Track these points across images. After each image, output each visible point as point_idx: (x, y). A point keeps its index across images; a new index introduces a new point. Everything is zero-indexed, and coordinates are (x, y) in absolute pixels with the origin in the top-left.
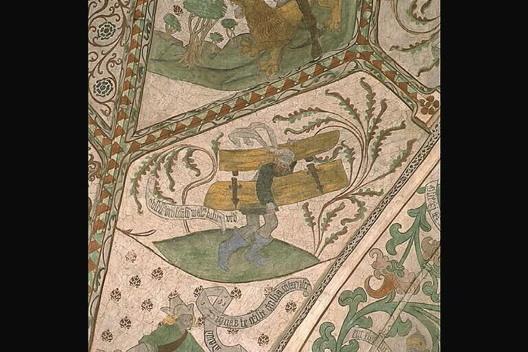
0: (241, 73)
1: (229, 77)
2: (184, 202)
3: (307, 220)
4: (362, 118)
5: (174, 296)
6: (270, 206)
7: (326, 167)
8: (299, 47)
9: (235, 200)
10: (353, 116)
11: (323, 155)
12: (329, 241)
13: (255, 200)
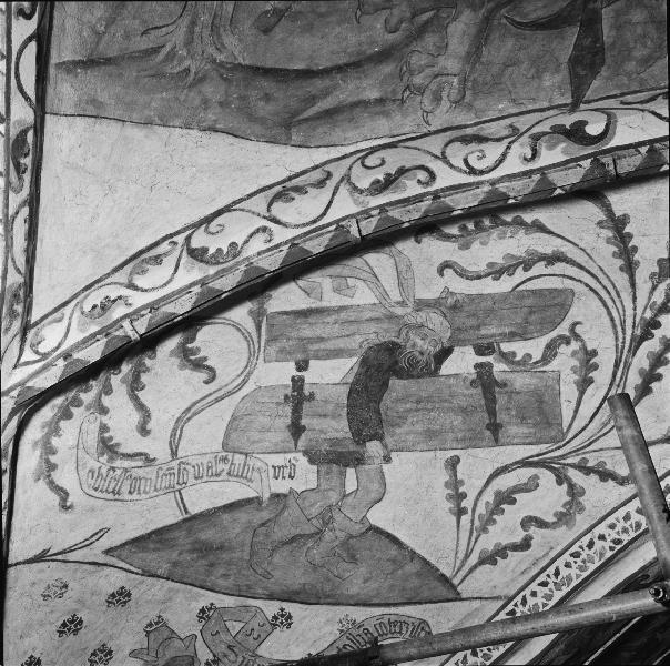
0: (351, 86)
1: (312, 100)
2: (174, 454)
3: (450, 497)
4: (642, 275)
5: (157, 627)
6: (373, 447)
7: (521, 381)
8: (537, 25)
9: (296, 429)
10: (620, 262)
11: (519, 348)
12: (489, 559)
13: (339, 428)
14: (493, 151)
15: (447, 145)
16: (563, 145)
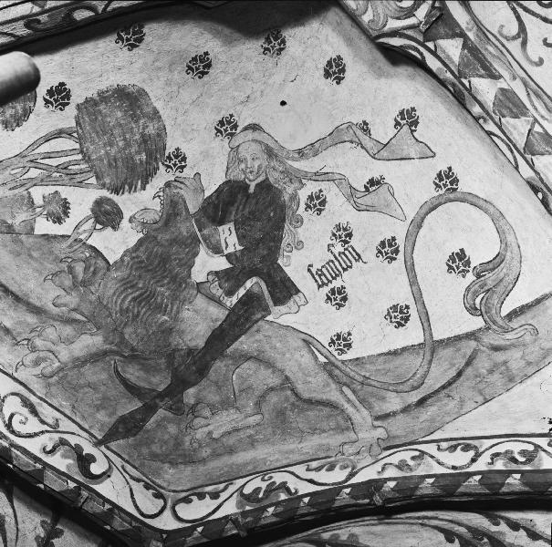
8: (125, 382)
14: (33, 425)
15: (13, 394)
16: (71, 461)
